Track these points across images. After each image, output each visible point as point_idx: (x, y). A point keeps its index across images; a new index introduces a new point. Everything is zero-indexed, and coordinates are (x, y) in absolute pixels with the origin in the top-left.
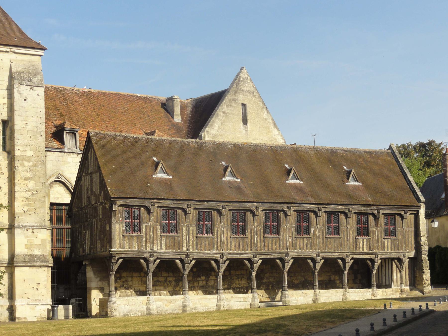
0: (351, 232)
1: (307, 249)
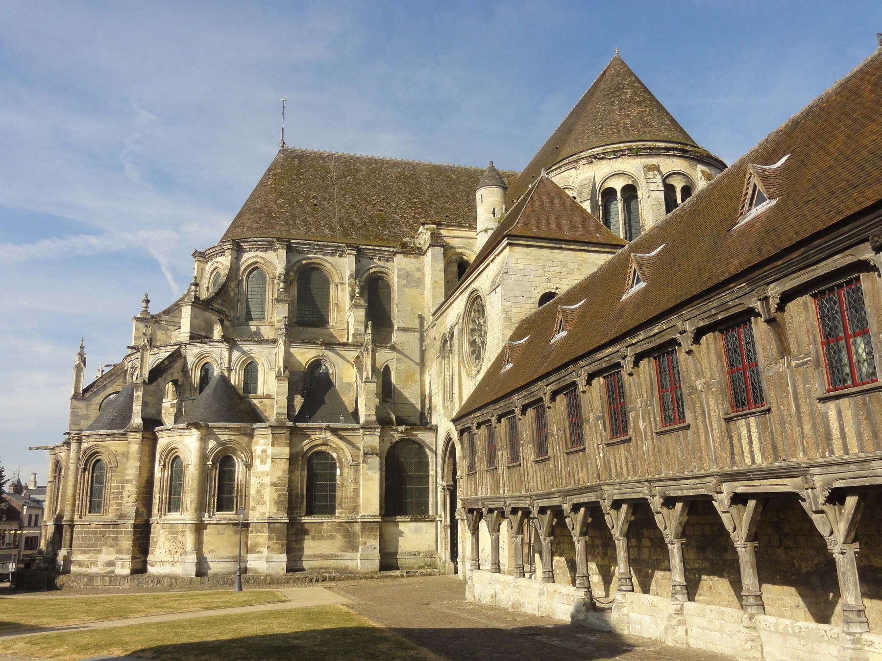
0: (712, 402)
1: (628, 475)
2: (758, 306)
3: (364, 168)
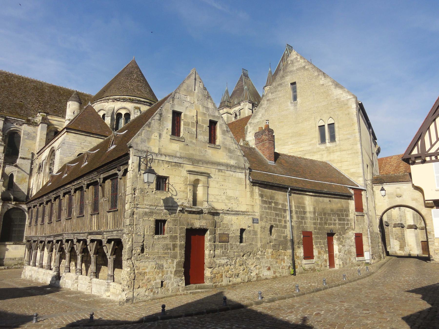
2: (98, 180)
3: (16, 80)
